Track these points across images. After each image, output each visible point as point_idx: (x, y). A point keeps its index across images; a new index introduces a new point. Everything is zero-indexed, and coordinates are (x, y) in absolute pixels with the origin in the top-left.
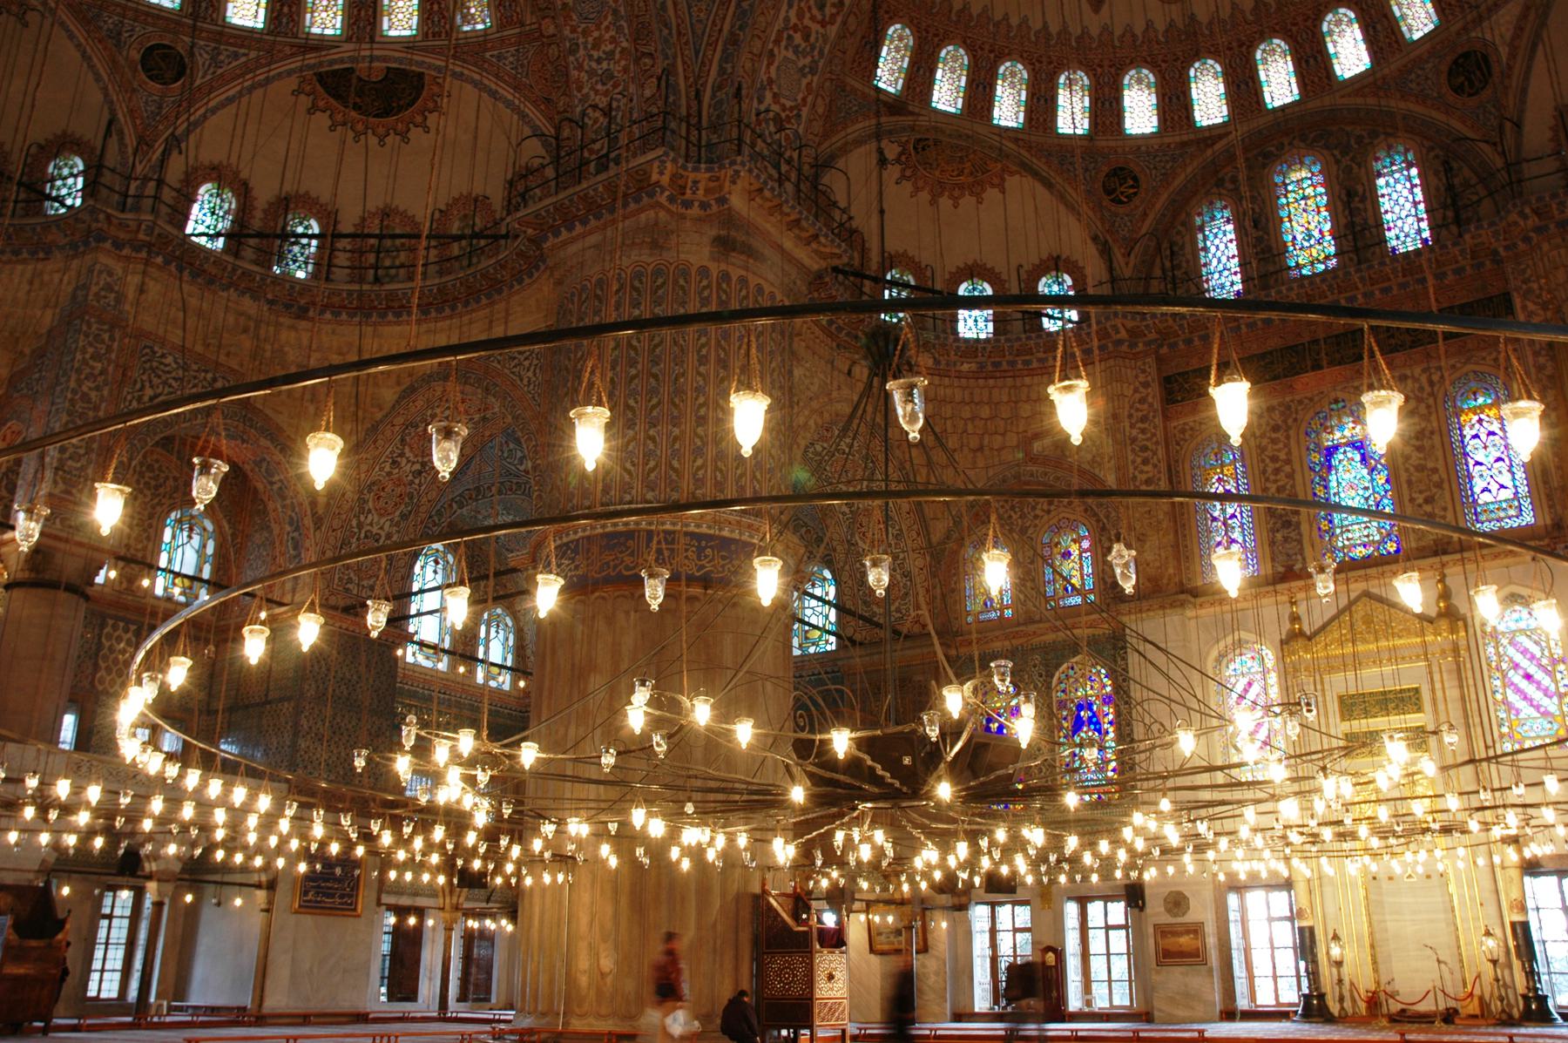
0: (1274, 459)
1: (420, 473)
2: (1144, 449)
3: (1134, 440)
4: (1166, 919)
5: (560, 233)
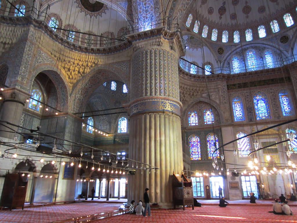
0: (248, 101)
1: (90, 87)
3: (222, 96)
4: (231, 181)
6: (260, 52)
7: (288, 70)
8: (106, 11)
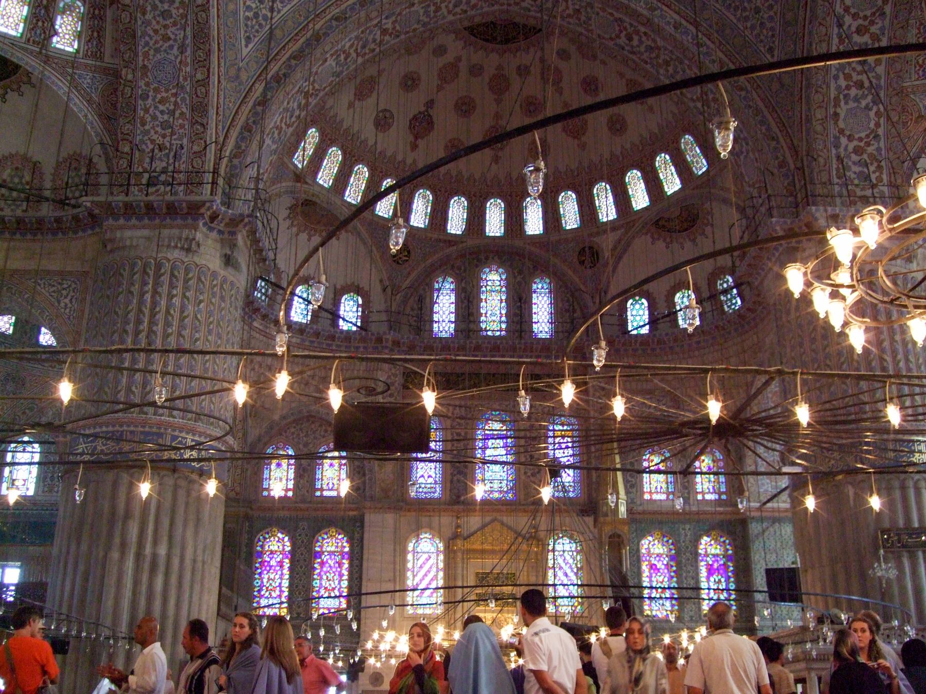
5: (118, 219)
6: (519, 279)
8: (24, 88)
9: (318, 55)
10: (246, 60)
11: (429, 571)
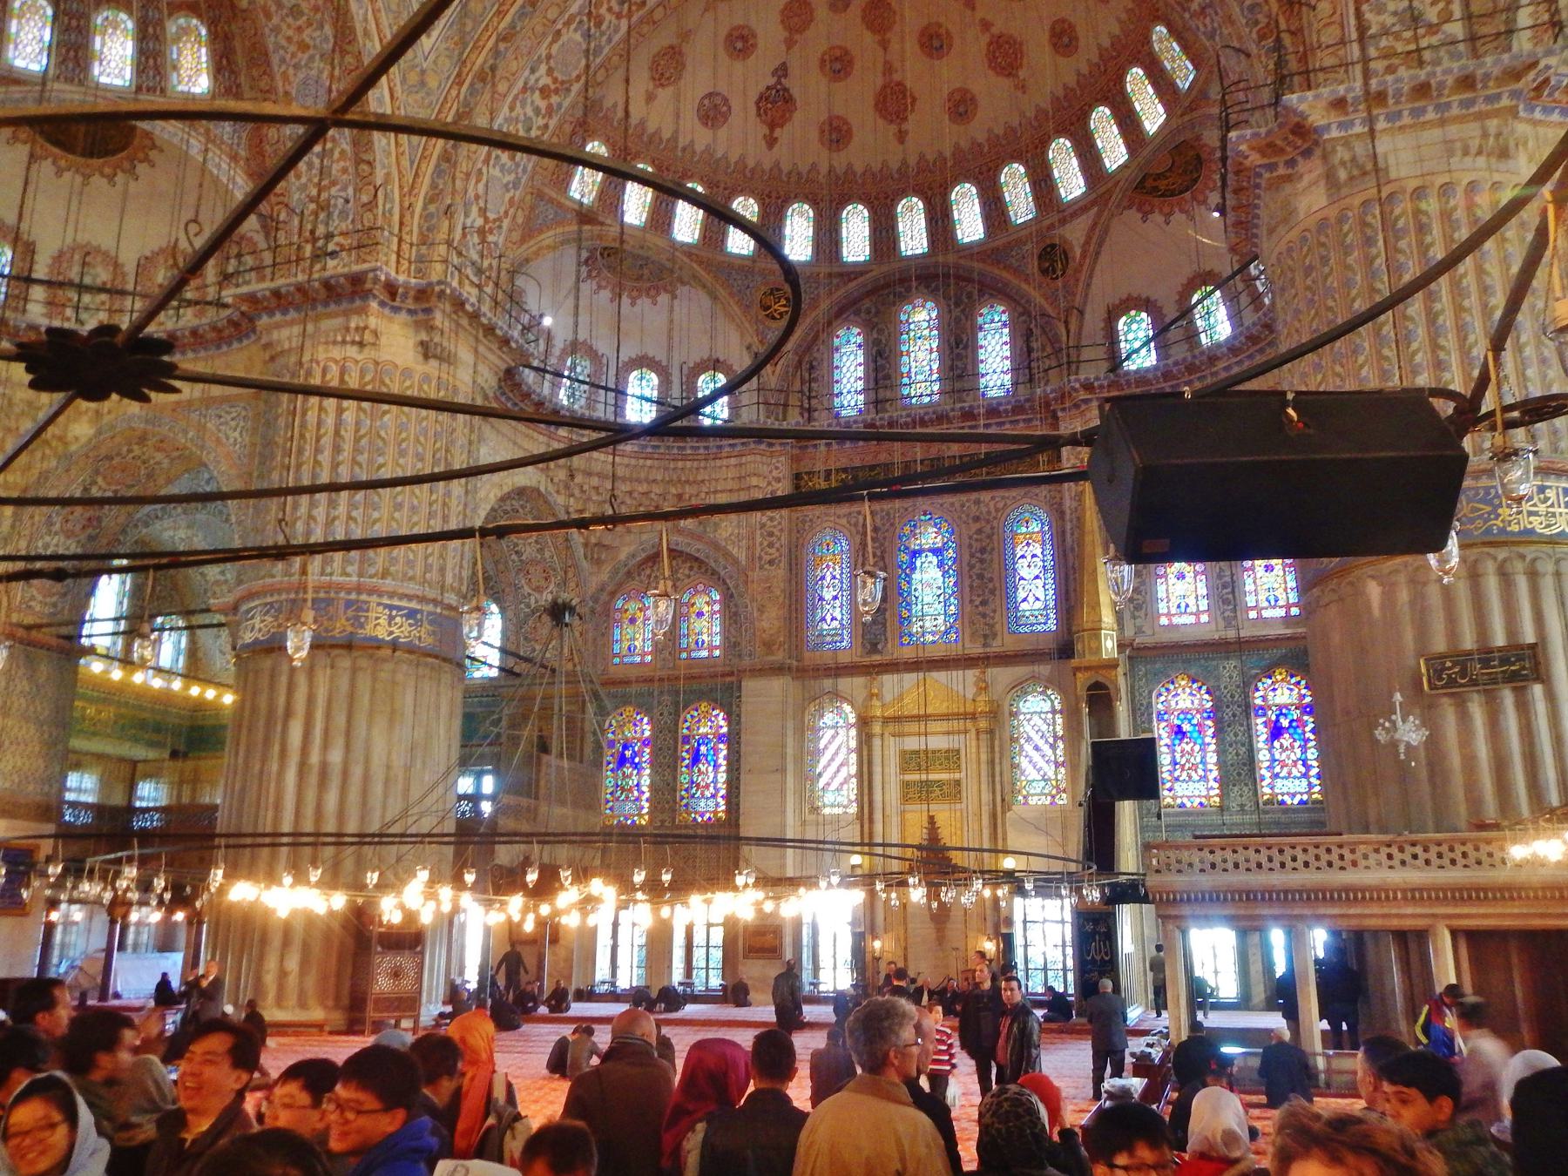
2: (771, 534)
3: (763, 526)
6: (957, 312)
7: (1054, 412)
9: (539, 29)
10: (432, 57)
11: (836, 753)
